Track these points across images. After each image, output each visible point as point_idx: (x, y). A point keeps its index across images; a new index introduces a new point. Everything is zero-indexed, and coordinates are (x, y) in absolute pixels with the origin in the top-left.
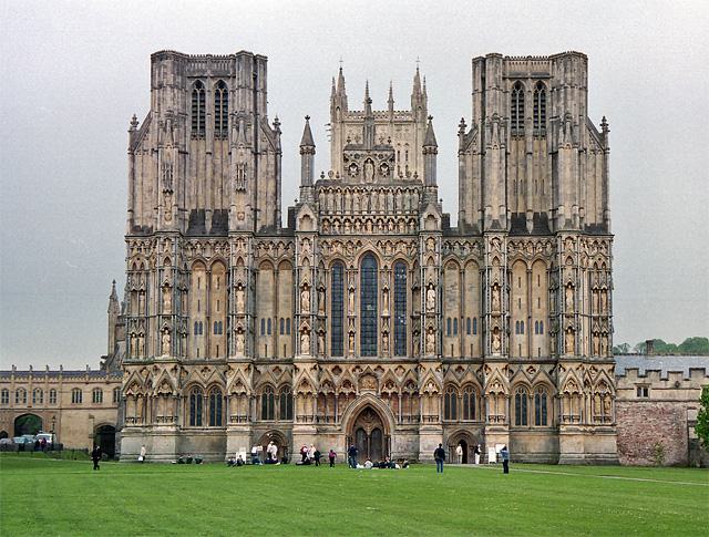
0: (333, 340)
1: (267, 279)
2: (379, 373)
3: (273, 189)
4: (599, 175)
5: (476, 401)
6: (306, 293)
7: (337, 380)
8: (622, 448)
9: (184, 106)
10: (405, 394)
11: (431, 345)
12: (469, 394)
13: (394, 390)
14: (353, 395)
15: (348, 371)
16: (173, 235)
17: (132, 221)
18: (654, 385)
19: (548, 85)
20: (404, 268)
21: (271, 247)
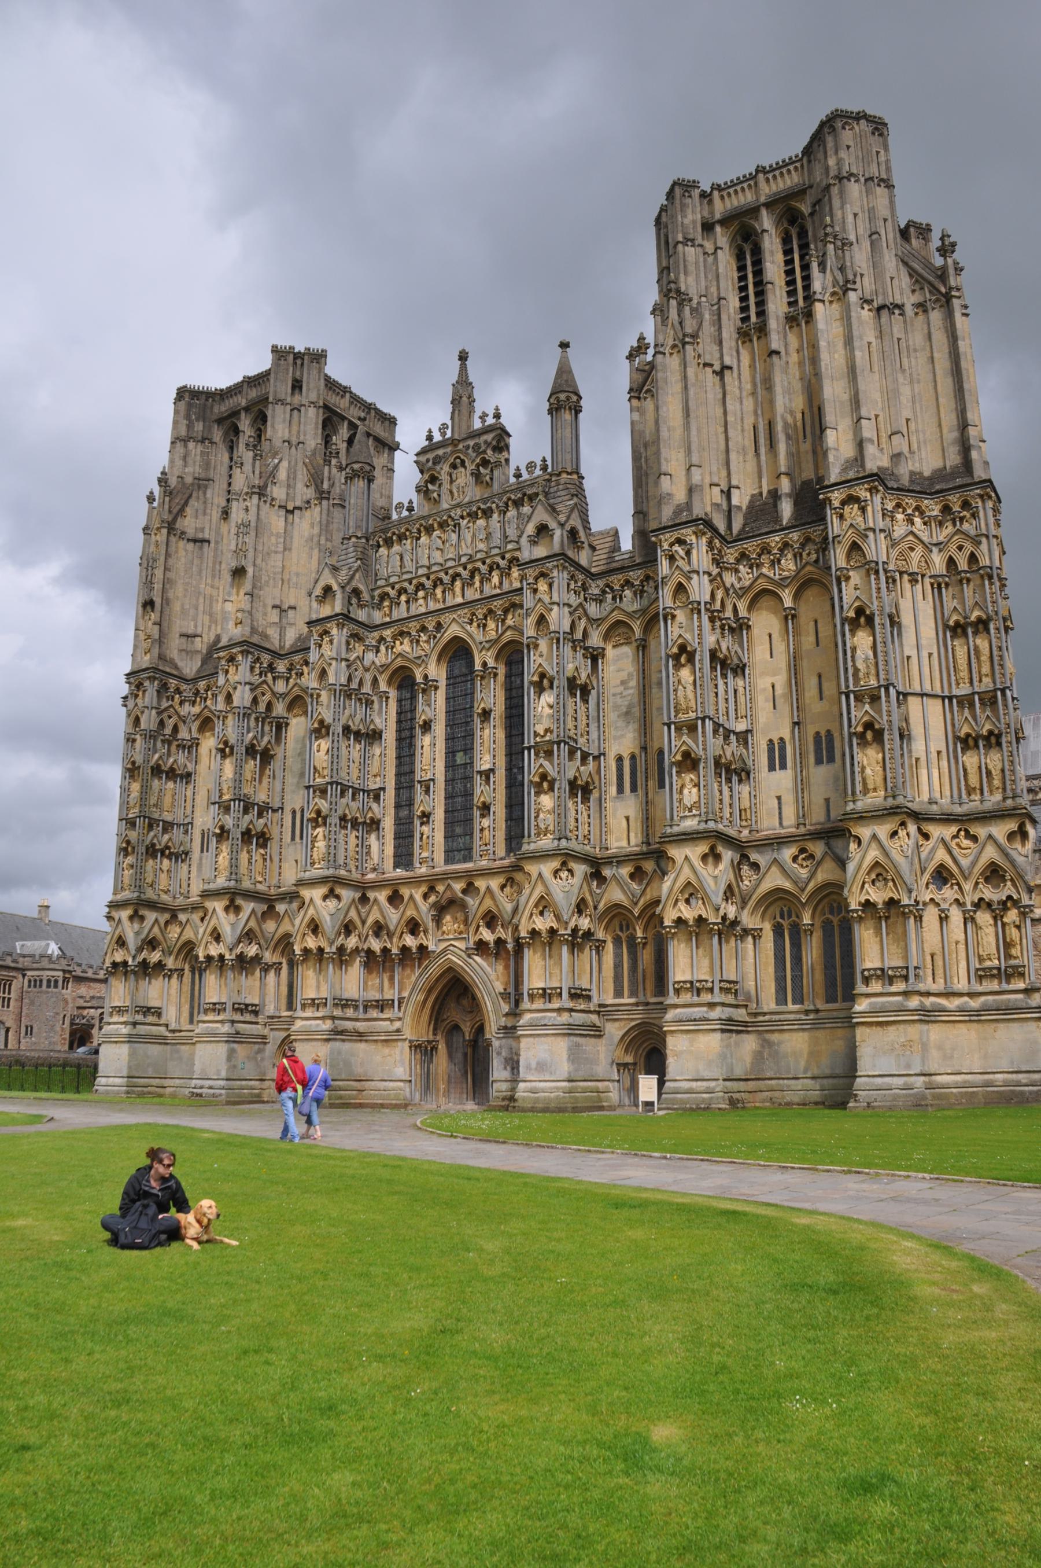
0: (397, 837)
6: (324, 744)
7: (393, 917)
9: (207, 465)
11: (547, 819)
13: (500, 932)
19: (805, 208)
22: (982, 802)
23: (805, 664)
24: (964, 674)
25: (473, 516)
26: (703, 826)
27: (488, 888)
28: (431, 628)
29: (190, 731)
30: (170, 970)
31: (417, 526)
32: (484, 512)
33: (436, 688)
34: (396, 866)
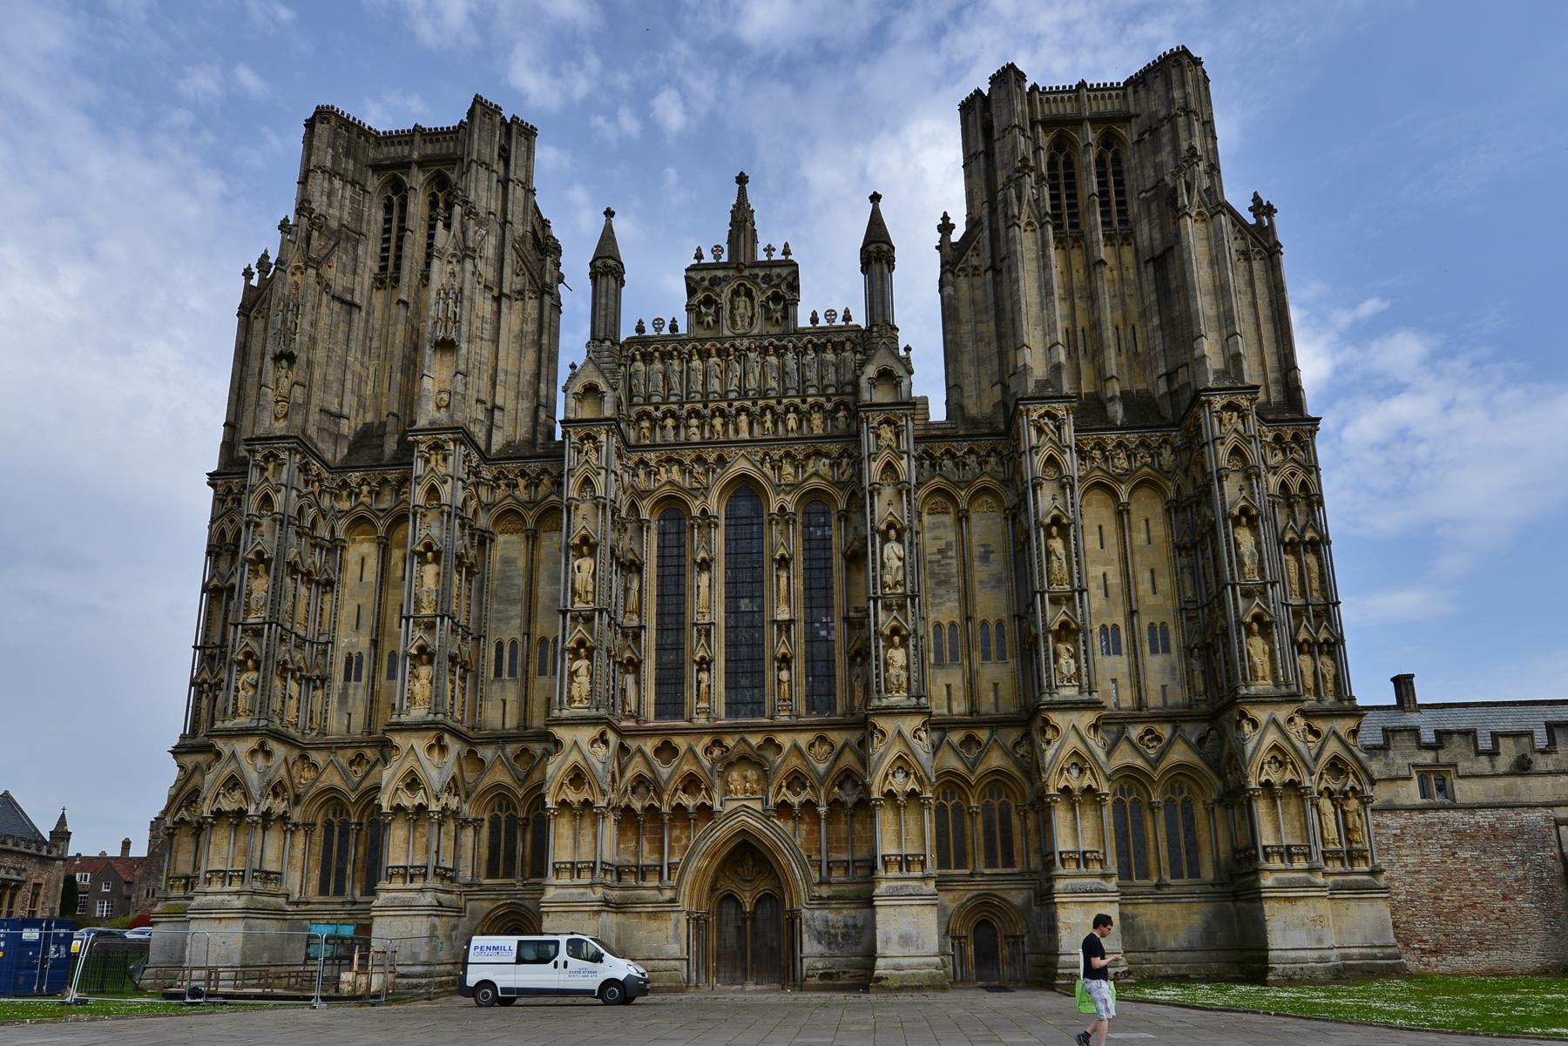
0: (659, 683)
1: (514, 554)
2: (769, 754)
3: (534, 367)
4: (1263, 302)
5: (1016, 821)
7: (664, 771)
8: (1404, 935)
9: (358, 216)
10: (834, 804)
12: (996, 803)
13: (805, 795)
14: (705, 811)
15: (696, 752)
17: (228, 446)
18: (1465, 766)
19: (1129, 134)
20: (826, 513)
21: (522, 482)
22: (1319, 700)
23: (1137, 557)
24: (1296, 587)
25: (764, 351)
27: (796, 747)
28: (711, 460)
29: (333, 531)
30: (296, 825)
31: (689, 347)
32: (776, 349)
33: (717, 526)
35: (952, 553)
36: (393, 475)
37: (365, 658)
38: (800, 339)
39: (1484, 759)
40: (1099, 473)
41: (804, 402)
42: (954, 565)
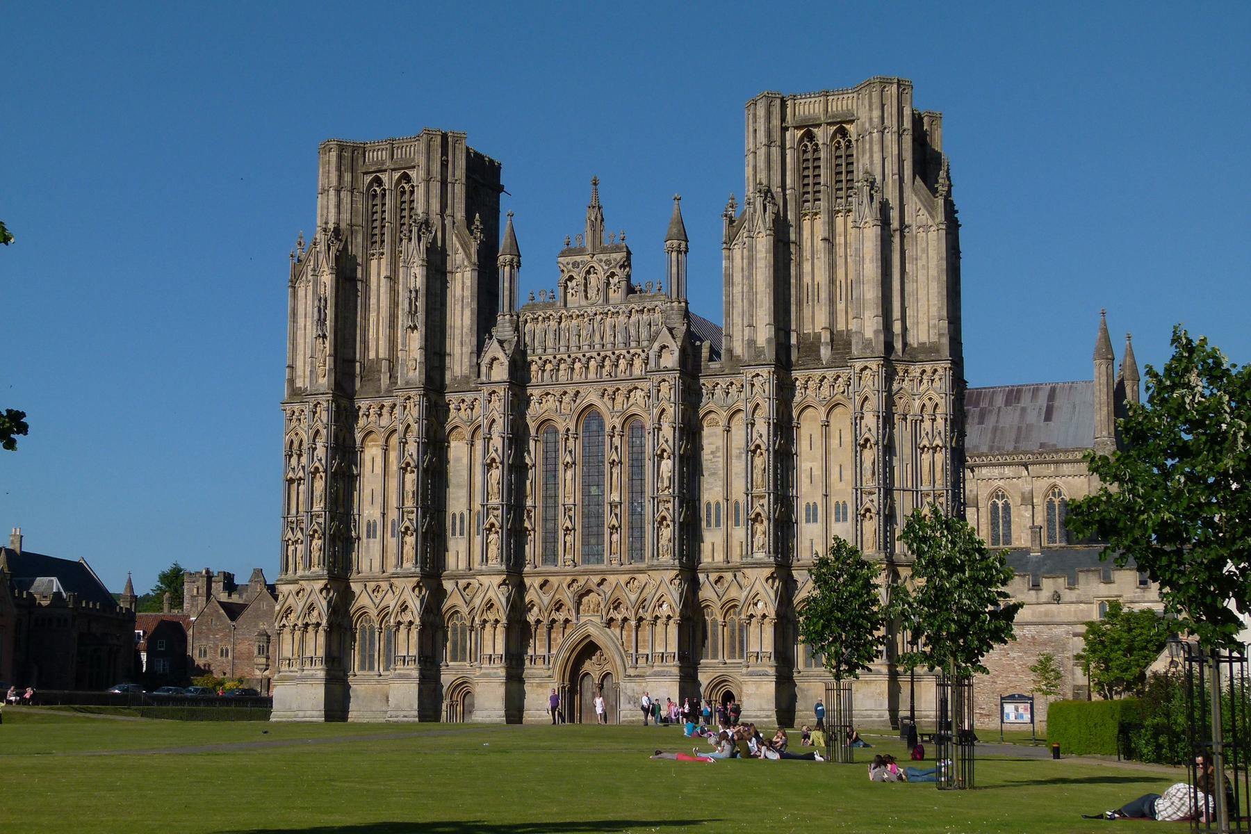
0: (545, 541)
16: (324, 397)
23: (832, 457)
26: (766, 560)
34: (545, 561)
35: (720, 454)
36: (387, 403)
37: (378, 523)
38: (628, 307)
39: (1033, 592)
40: (811, 399)
41: (628, 352)
42: (720, 462)
